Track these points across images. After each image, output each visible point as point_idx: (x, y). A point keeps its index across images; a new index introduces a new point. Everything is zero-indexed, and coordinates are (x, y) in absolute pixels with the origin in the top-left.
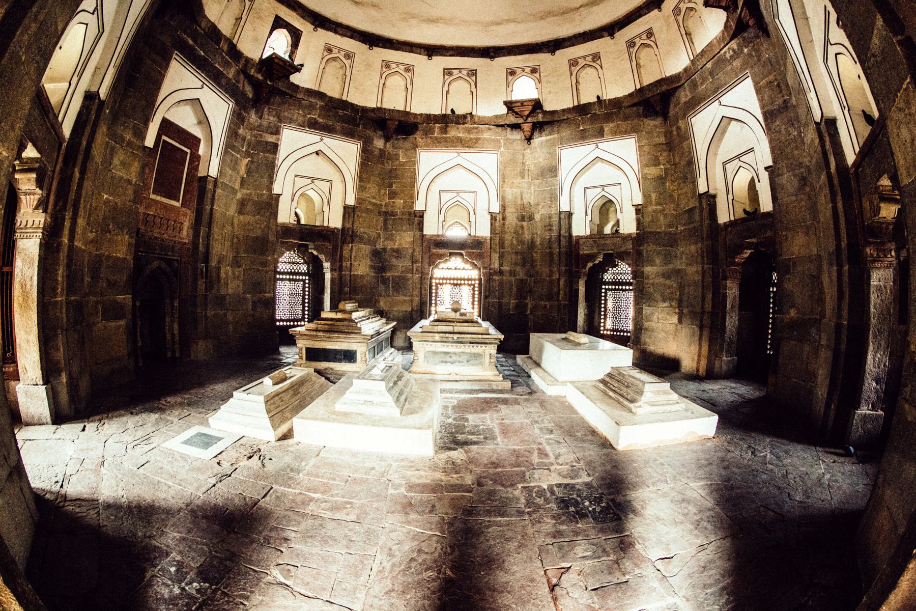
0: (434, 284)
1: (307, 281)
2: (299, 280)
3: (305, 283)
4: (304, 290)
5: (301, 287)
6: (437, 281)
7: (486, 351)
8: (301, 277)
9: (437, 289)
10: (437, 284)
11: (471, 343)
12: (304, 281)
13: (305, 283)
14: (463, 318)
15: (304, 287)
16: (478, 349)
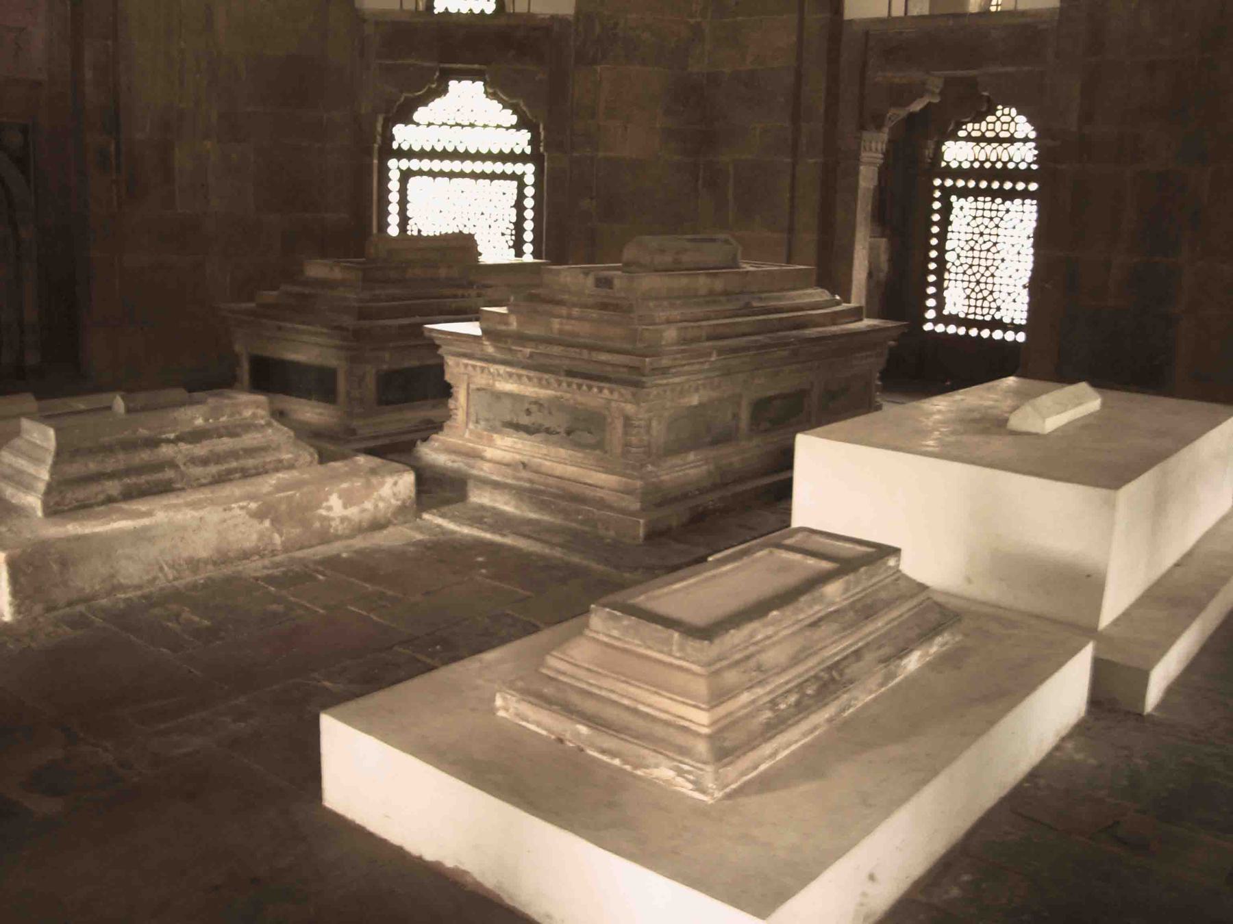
0: (937, 194)
1: (529, 179)
2: (503, 176)
3: (521, 186)
4: (519, 206)
5: (512, 197)
6: (949, 183)
7: (614, 404)
8: (509, 168)
9: (947, 209)
10: (947, 192)
11: (571, 373)
12: (519, 179)
13: (521, 186)
14: (603, 292)
15: (521, 196)
16: (595, 397)
